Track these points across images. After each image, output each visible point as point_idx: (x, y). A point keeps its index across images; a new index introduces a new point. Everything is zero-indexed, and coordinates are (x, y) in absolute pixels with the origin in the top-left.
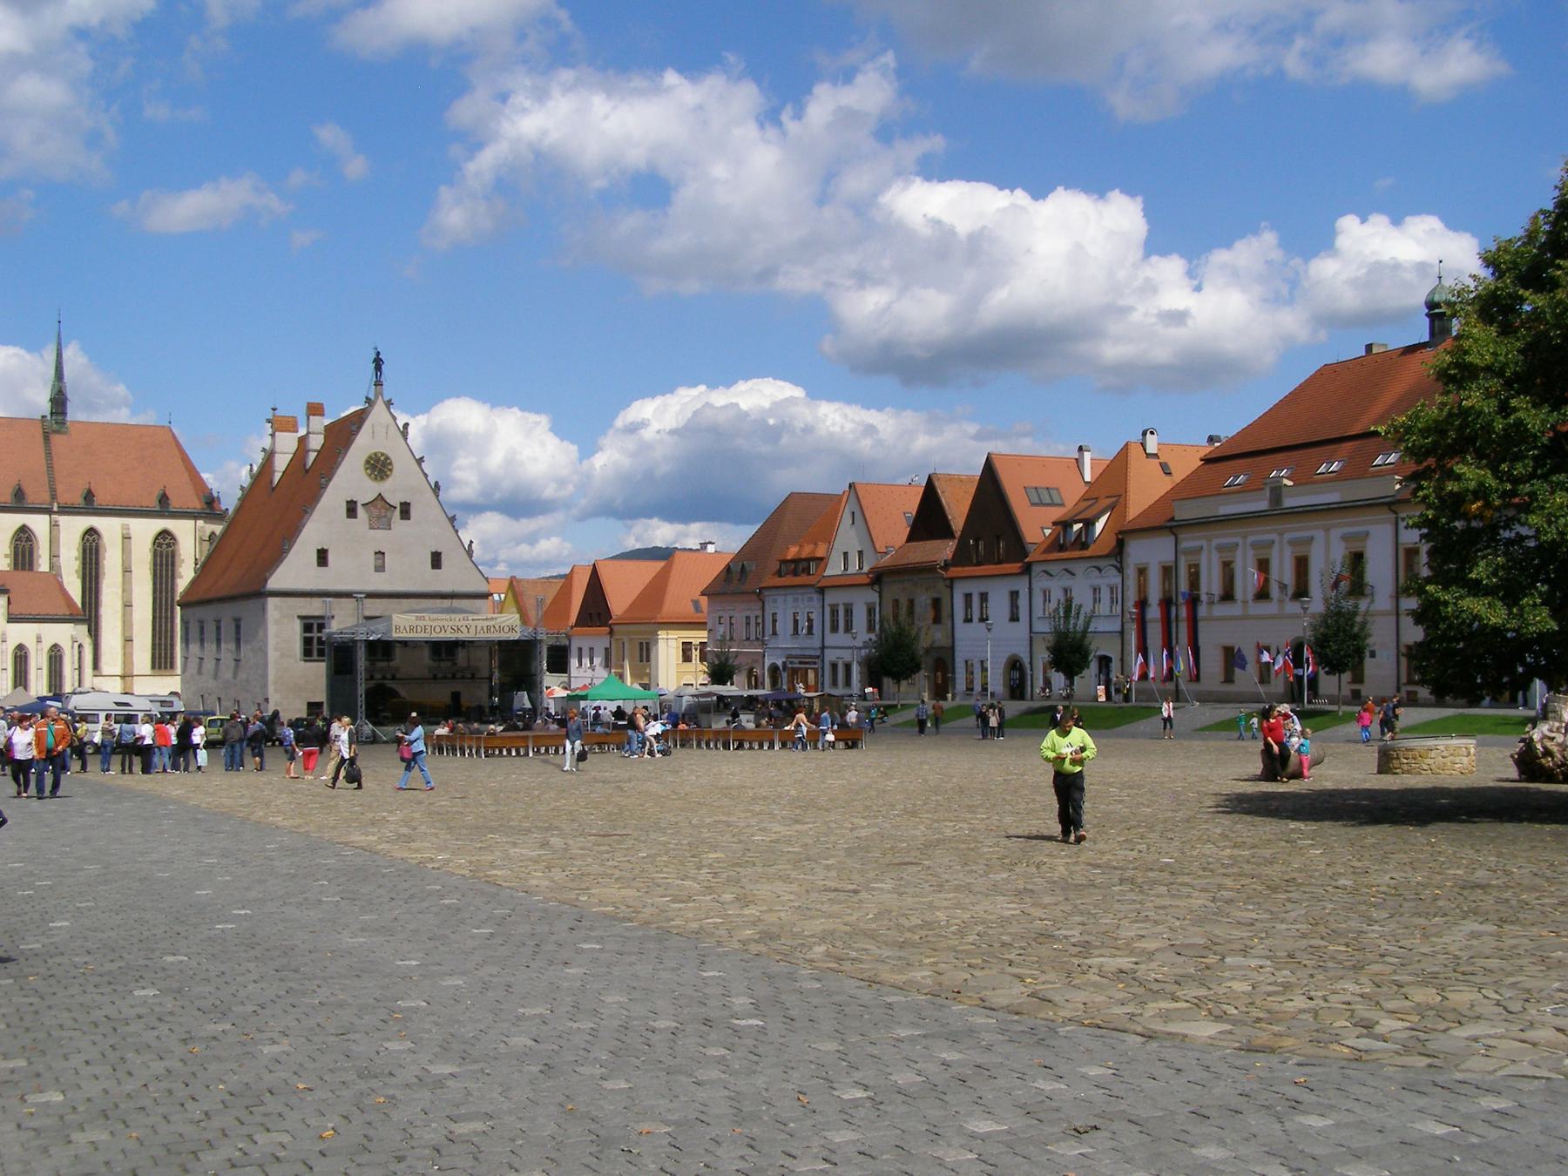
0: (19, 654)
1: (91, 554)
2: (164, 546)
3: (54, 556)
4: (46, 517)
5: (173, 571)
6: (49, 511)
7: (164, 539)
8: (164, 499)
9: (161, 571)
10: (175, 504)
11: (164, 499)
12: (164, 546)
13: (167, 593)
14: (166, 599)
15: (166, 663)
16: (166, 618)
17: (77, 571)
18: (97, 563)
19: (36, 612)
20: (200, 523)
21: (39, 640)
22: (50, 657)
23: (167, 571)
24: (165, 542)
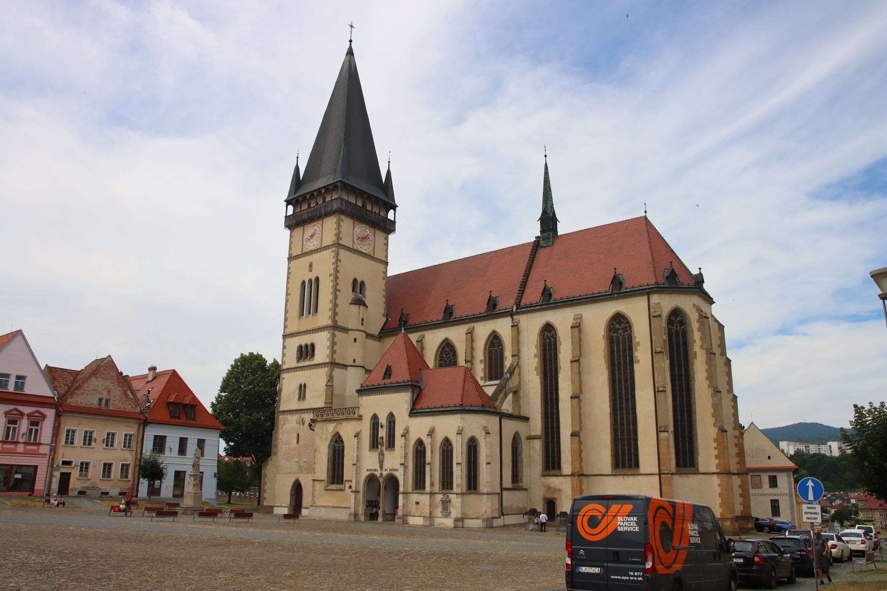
0: (419, 448)
1: (550, 350)
2: (620, 331)
3: (516, 355)
4: (509, 319)
5: (631, 356)
6: (511, 314)
7: (620, 323)
8: (617, 282)
9: (619, 357)
10: (628, 284)
11: (617, 282)
12: (620, 331)
13: (626, 381)
14: (626, 388)
15: (630, 460)
16: (627, 409)
17: (536, 369)
18: (556, 359)
19: (432, 406)
20: (655, 299)
21: (431, 433)
22: (444, 451)
23: (625, 356)
24: (619, 325)
